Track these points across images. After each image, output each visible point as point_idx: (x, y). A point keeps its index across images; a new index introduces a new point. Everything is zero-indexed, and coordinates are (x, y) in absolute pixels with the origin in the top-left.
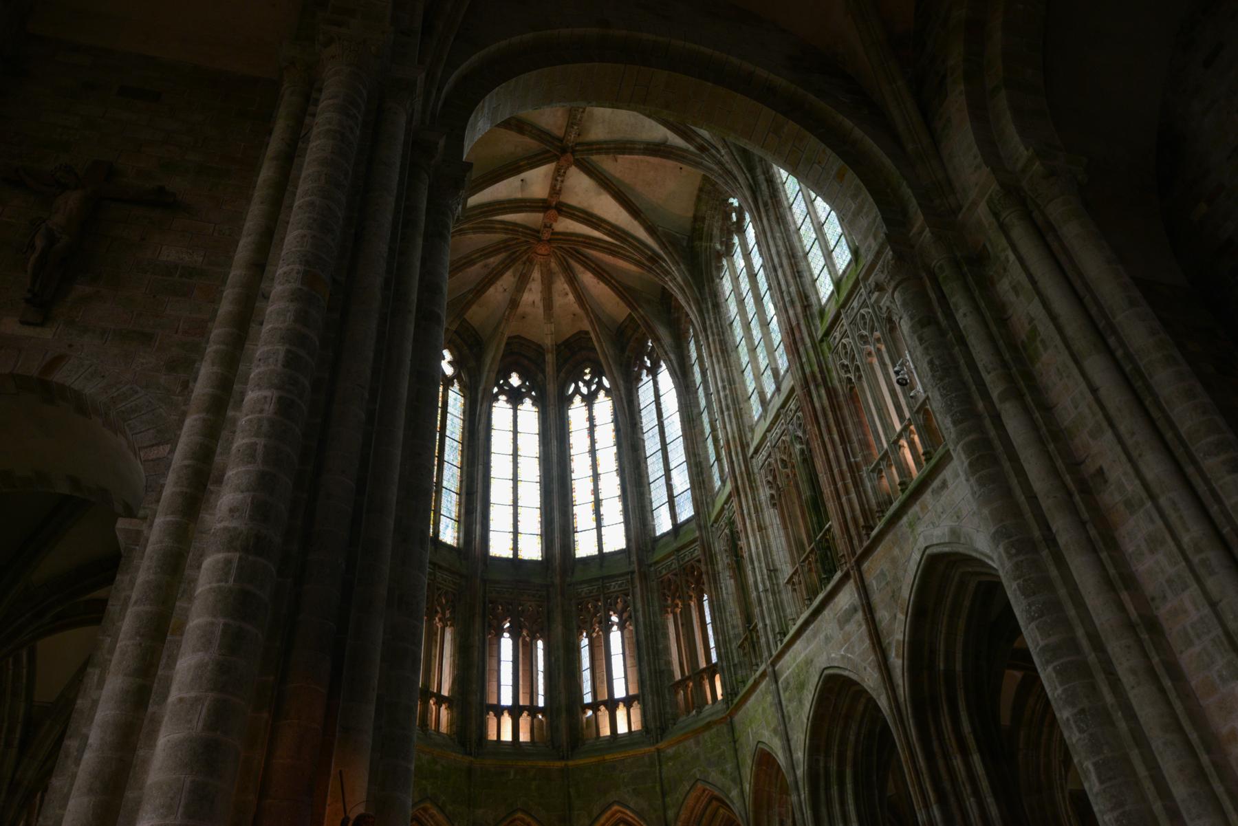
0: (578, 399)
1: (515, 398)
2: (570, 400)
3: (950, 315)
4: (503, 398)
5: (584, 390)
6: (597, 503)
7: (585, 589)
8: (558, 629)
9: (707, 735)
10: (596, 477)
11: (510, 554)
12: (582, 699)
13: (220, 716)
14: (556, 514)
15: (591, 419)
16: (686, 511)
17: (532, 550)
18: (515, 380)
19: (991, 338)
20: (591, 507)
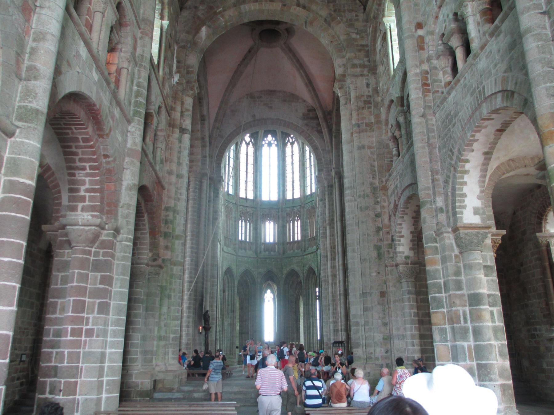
0: (289, 143)
1: (270, 144)
2: (286, 145)
3: (325, 199)
4: (266, 145)
5: (291, 140)
6: (293, 182)
7: (288, 210)
8: (281, 222)
9: (312, 255)
10: (293, 173)
11: (267, 199)
12: (286, 240)
13: (190, 303)
14: (281, 186)
15: (292, 152)
16: (314, 191)
17: (274, 198)
18: (270, 138)
19: (329, 209)
20: (291, 183)
